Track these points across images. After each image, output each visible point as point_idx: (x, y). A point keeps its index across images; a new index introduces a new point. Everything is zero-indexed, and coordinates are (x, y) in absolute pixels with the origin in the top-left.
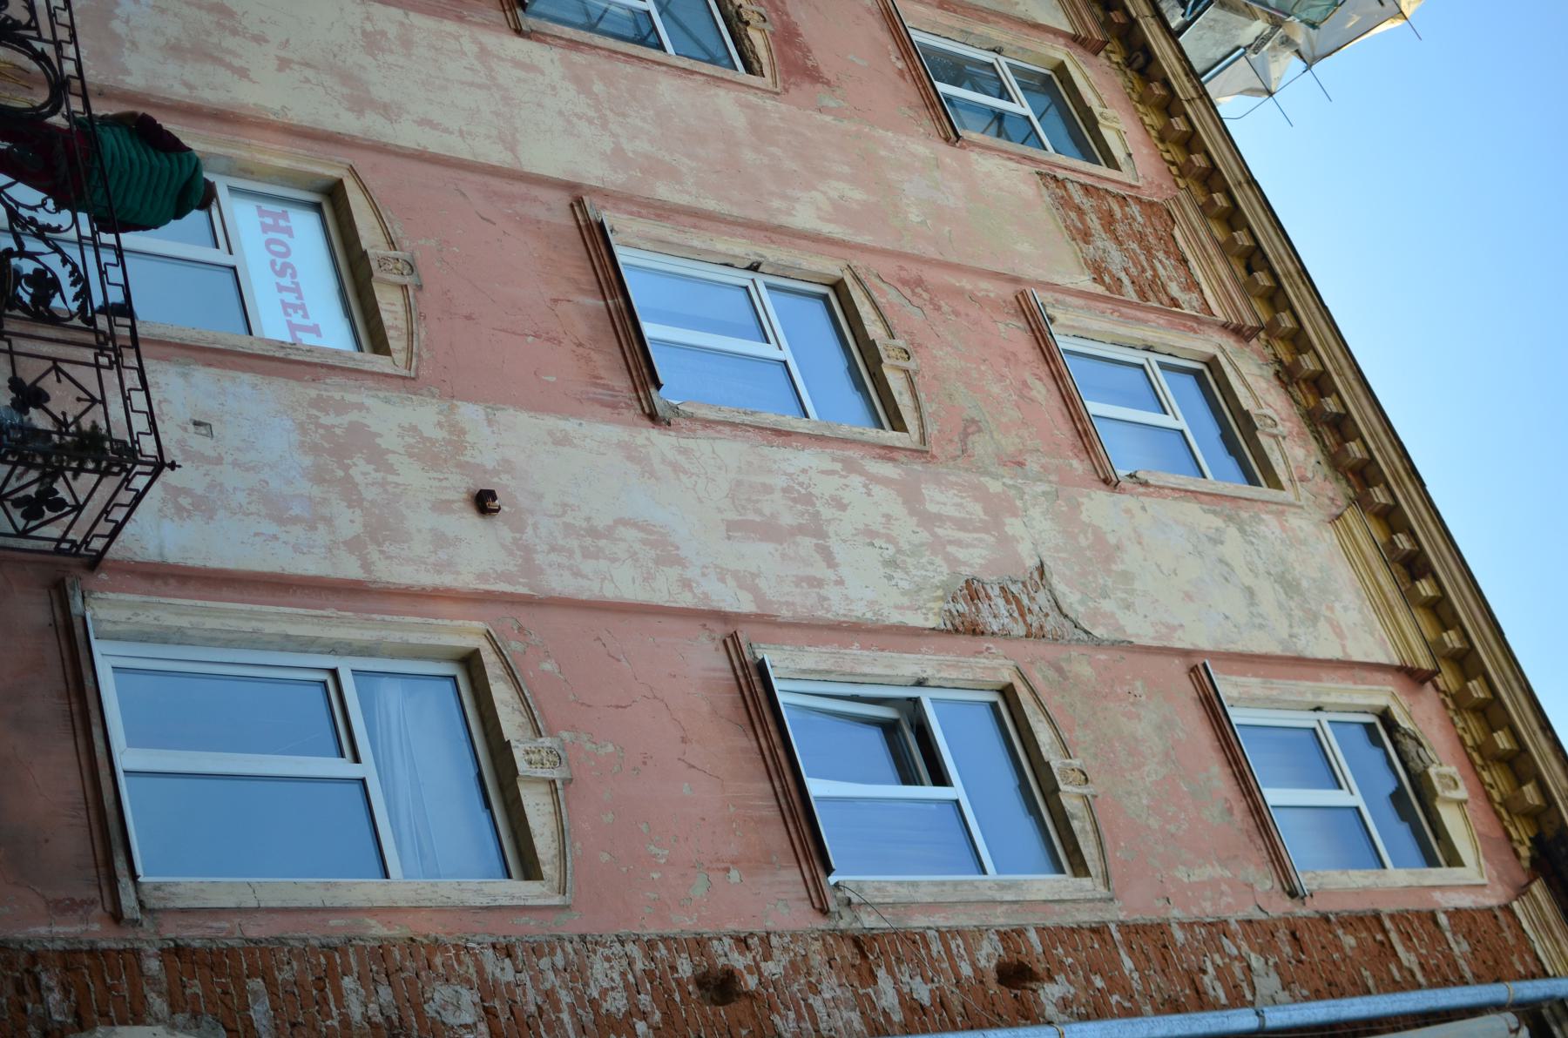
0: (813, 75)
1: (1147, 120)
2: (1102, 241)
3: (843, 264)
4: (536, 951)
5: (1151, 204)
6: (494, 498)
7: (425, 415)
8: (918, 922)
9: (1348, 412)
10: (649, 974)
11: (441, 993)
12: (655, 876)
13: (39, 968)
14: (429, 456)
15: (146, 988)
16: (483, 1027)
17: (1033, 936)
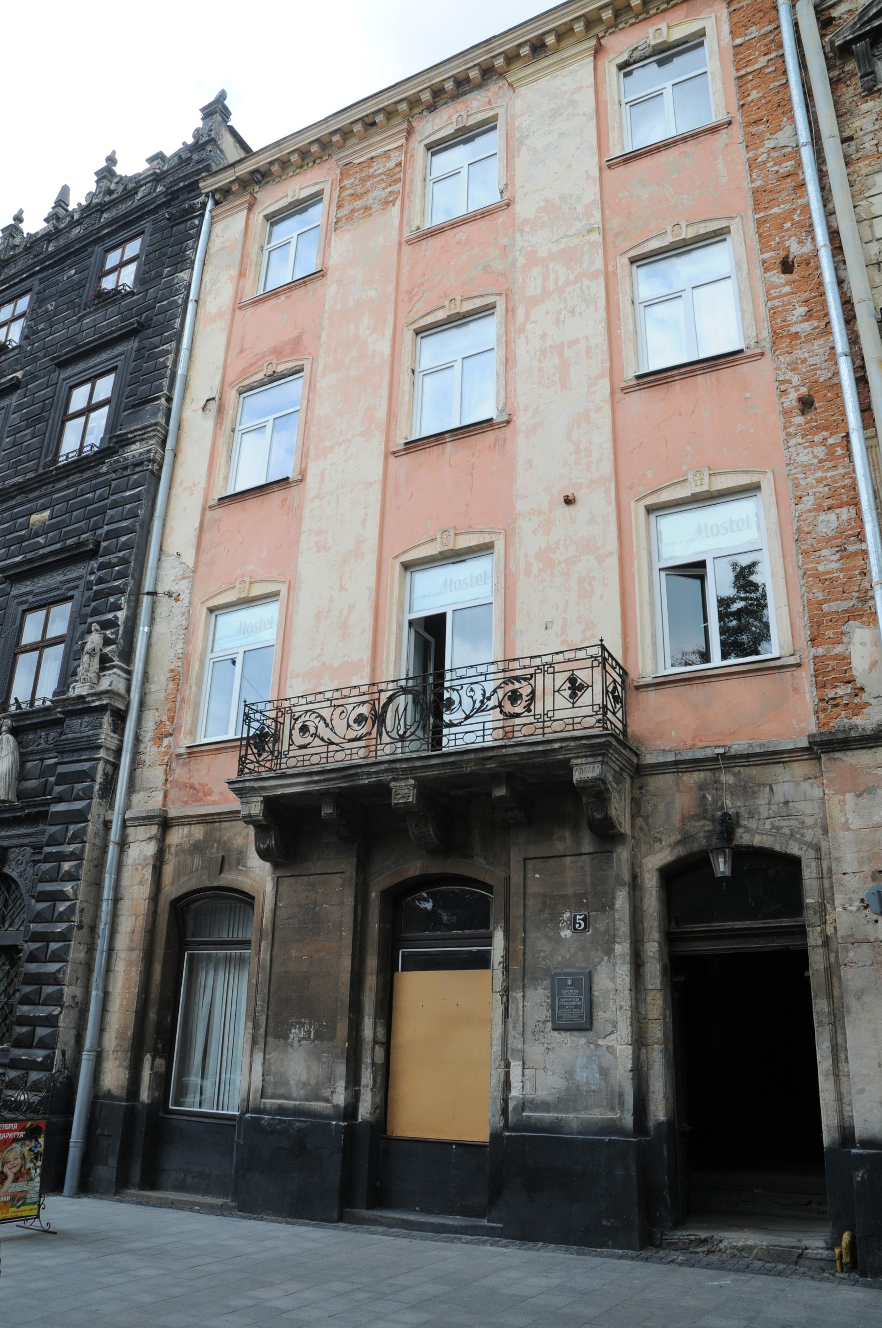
1: (291, 174)
2: (369, 200)
3: (405, 329)
5: (341, 174)
6: (568, 496)
7: (526, 527)
8: (763, 311)
9: (452, 76)
12: (752, 431)
13: (826, 698)
15: (832, 653)
16: (838, 511)
17: (766, 256)
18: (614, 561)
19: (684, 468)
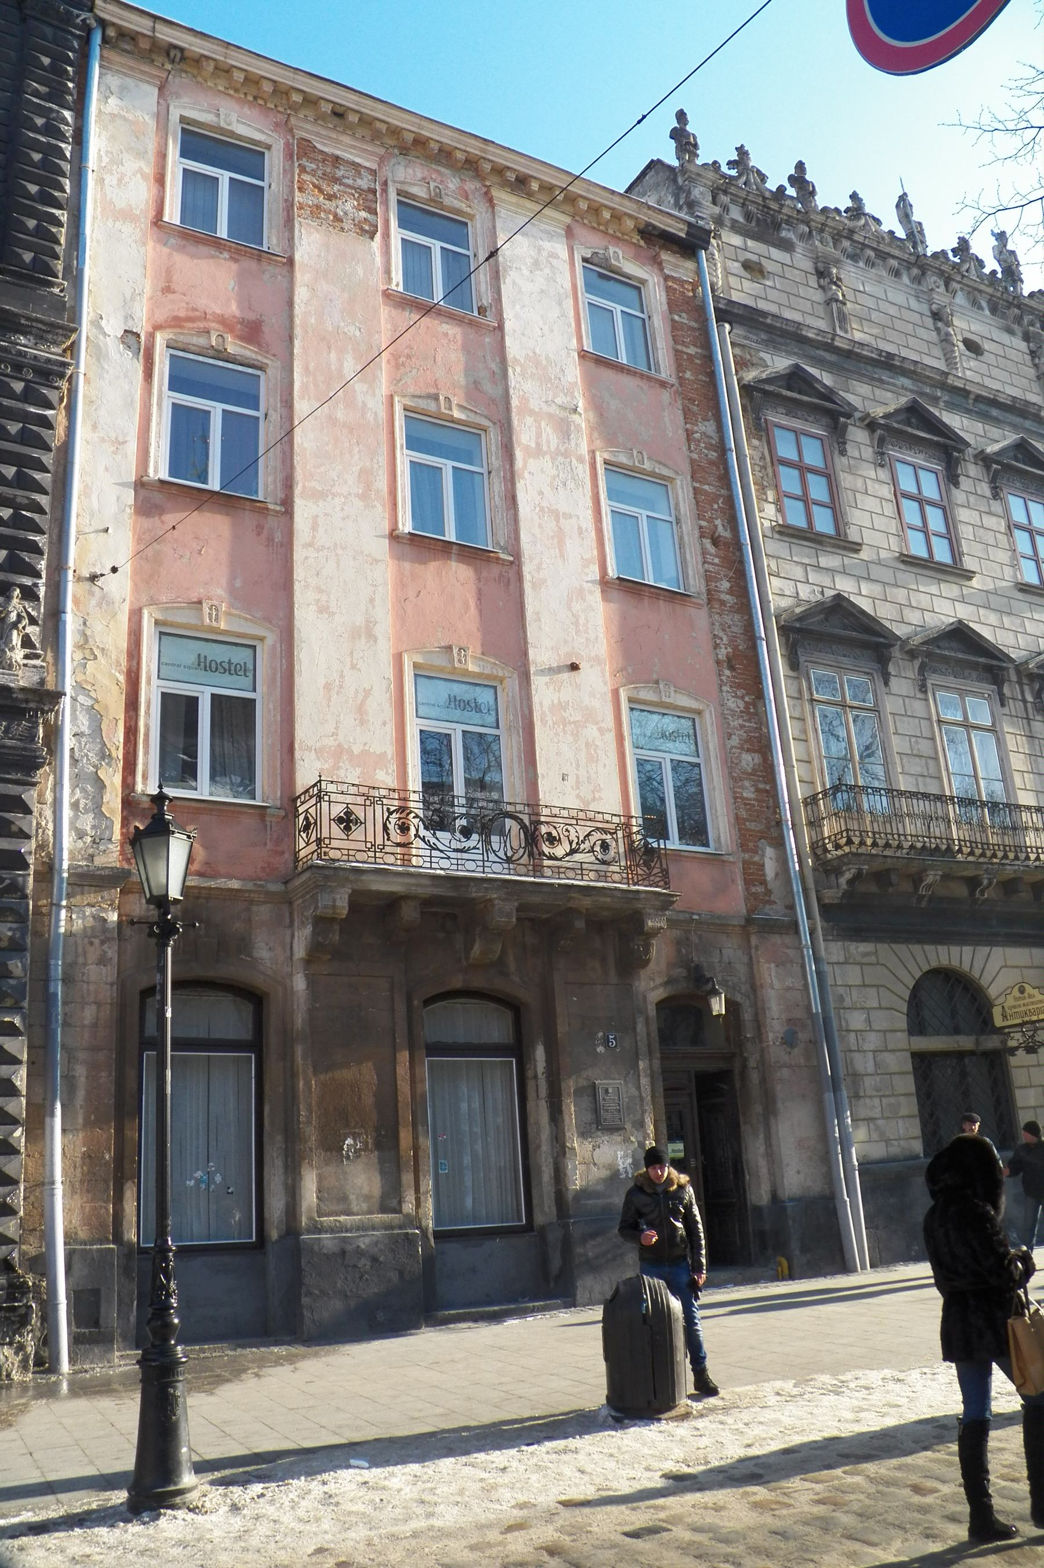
4: (729, 724)
10: (731, 687)
11: (744, 763)
18: (611, 737)
19: (655, 676)
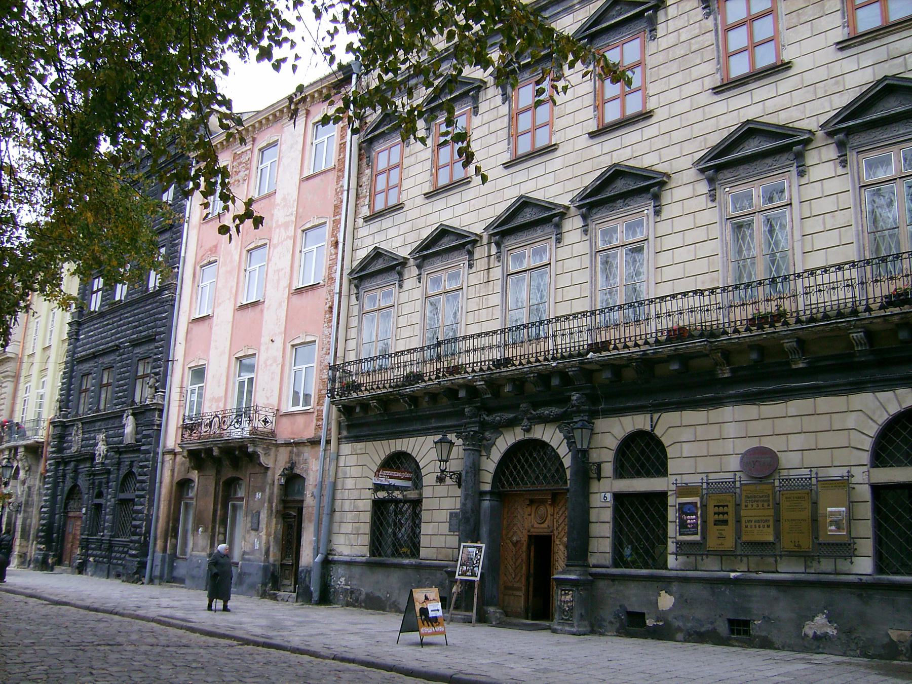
0: (216, 246)
7: (263, 348)
14: (267, 349)
